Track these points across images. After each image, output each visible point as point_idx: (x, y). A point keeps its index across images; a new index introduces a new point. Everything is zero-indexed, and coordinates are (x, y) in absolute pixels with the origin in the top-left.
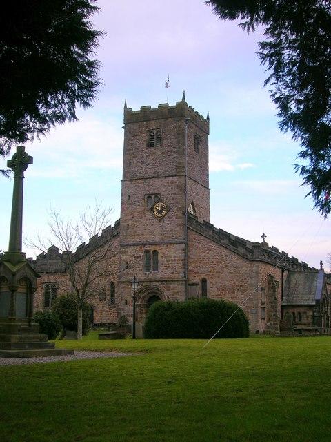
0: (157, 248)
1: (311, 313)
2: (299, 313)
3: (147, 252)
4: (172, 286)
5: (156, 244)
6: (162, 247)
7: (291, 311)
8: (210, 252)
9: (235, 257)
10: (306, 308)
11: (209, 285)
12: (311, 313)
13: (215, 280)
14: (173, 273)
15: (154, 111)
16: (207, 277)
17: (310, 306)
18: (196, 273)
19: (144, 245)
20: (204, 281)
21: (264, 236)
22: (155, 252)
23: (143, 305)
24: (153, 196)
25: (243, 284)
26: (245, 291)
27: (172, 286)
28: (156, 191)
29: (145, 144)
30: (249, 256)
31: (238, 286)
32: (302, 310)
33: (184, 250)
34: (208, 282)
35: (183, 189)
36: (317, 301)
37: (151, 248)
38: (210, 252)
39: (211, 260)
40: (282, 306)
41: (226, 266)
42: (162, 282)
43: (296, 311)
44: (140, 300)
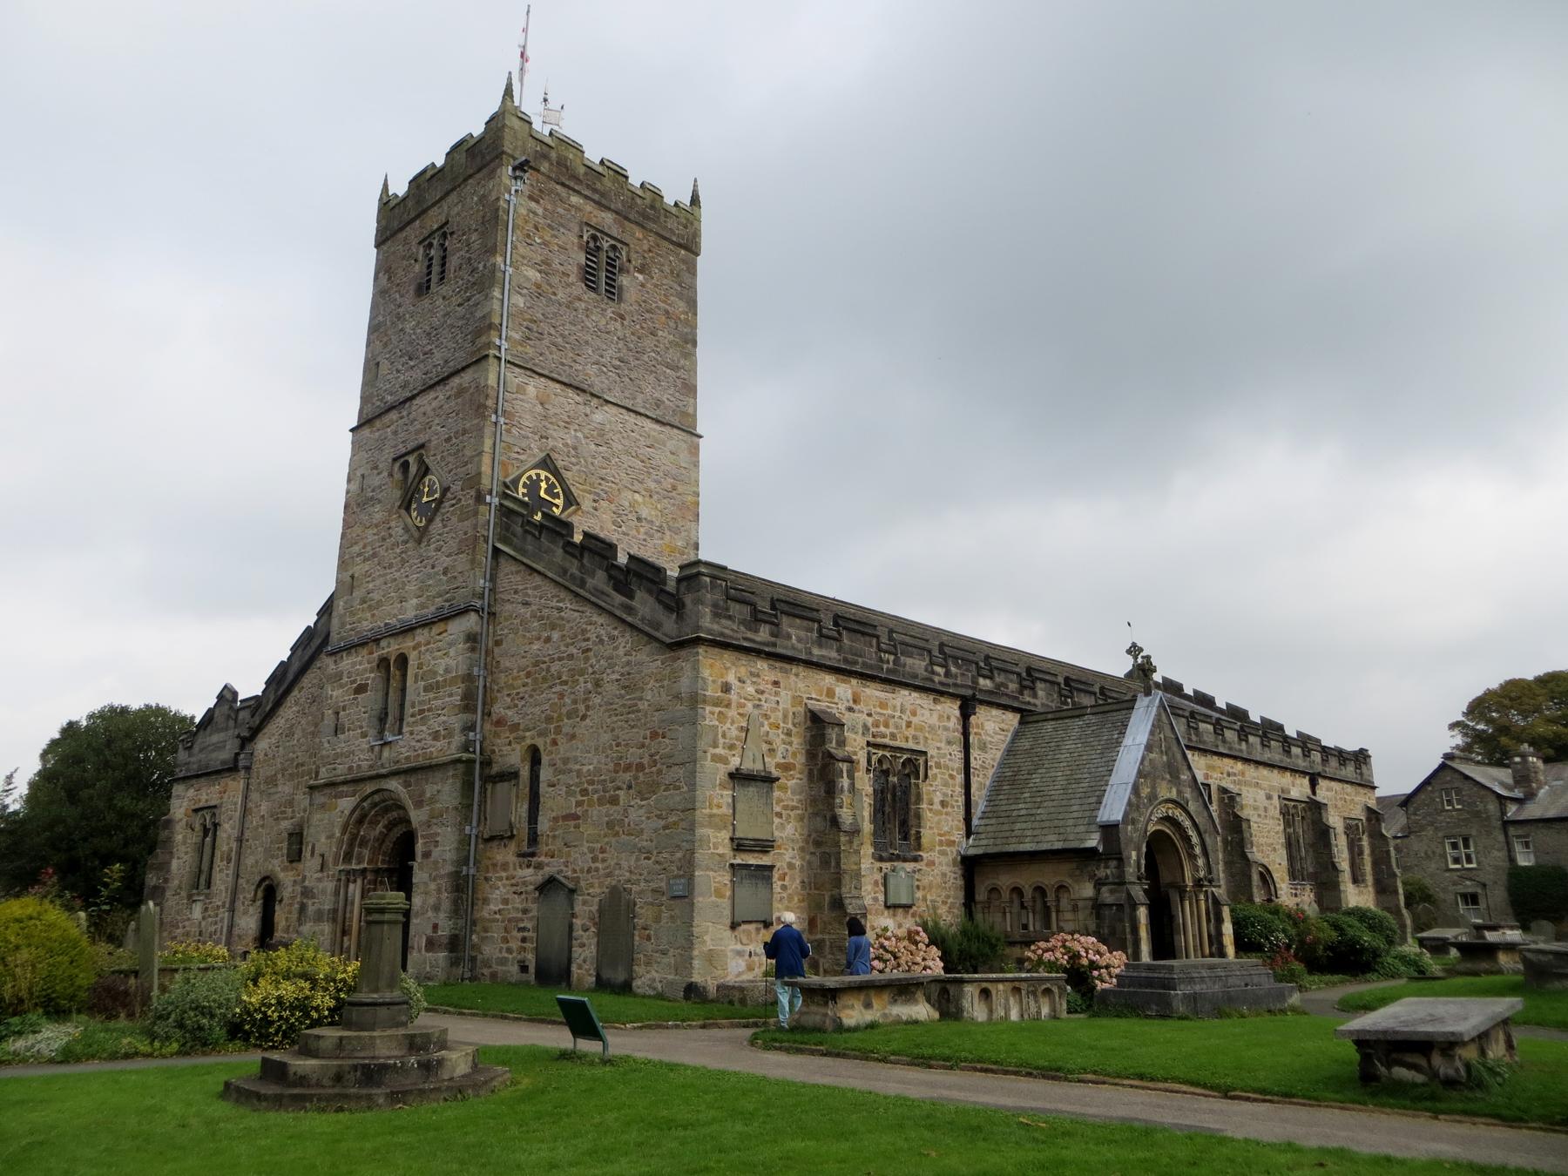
0: (406, 645)
1: (1088, 890)
2: (1040, 891)
3: (383, 663)
4: (430, 790)
5: (408, 630)
6: (421, 636)
7: (1005, 880)
8: (556, 635)
9: (625, 641)
10: (1066, 867)
11: (545, 774)
12: (1088, 890)
13: (563, 747)
14: (436, 736)
15: (442, 169)
16: (540, 742)
17: (1083, 857)
18: (515, 727)
19: (377, 641)
20: (535, 756)
21: (1134, 650)
22: (403, 660)
23: (377, 871)
24: (411, 459)
25: (645, 761)
26: (653, 787)
27: (430, 790)
28: (422, 439)
29: (412, 288)
30: (670, 627)
31: (628, 768)
32: (1048, 877)
33: (472, 638)
34: (545, 759)
35: (478, 405)
36: (1110, 830)
37: (391, 648)
38: (556, 635)
39: (555, 667)
40: (971, 866)
41: (597, 684)
42: (406, 772)
43: (1026, 879)
44: (366, 853)
